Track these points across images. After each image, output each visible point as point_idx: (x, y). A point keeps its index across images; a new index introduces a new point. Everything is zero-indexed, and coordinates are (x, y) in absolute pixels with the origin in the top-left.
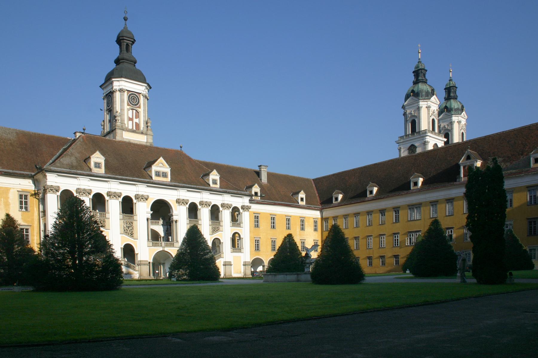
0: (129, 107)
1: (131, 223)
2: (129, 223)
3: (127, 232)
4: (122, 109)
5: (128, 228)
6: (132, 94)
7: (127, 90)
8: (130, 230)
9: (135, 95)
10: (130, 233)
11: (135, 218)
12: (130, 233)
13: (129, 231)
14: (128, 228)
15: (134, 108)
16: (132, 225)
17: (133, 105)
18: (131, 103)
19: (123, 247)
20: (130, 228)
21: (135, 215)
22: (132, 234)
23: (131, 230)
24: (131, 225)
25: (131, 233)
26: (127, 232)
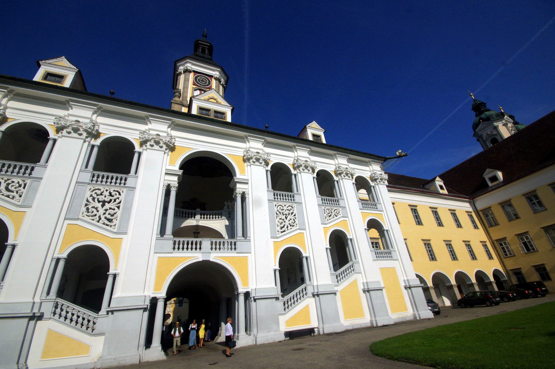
0: (195, 86)
1: (113, 193)
2: (110, 193)
3: (95, 215)
4: (186, 87)
5: (103, 206)
6: (201, 76)
7: (194, 71)
8: (106, 210)
9: (205, 77)
10: (106, 218)
11: (130, 182)
12: (106, 218)
13: (102, 211)
14: (103, 206)
15: (202, 88)
16: (118, 198)
17: (201, 85)
18: (198, 83)
19: (65, 255)
20: (107, 206)
21: (132, 176)
22: (110, 220)
23: (110, 209)
24: (115, 197)
25: (109, 217)
26: (95, 215)
